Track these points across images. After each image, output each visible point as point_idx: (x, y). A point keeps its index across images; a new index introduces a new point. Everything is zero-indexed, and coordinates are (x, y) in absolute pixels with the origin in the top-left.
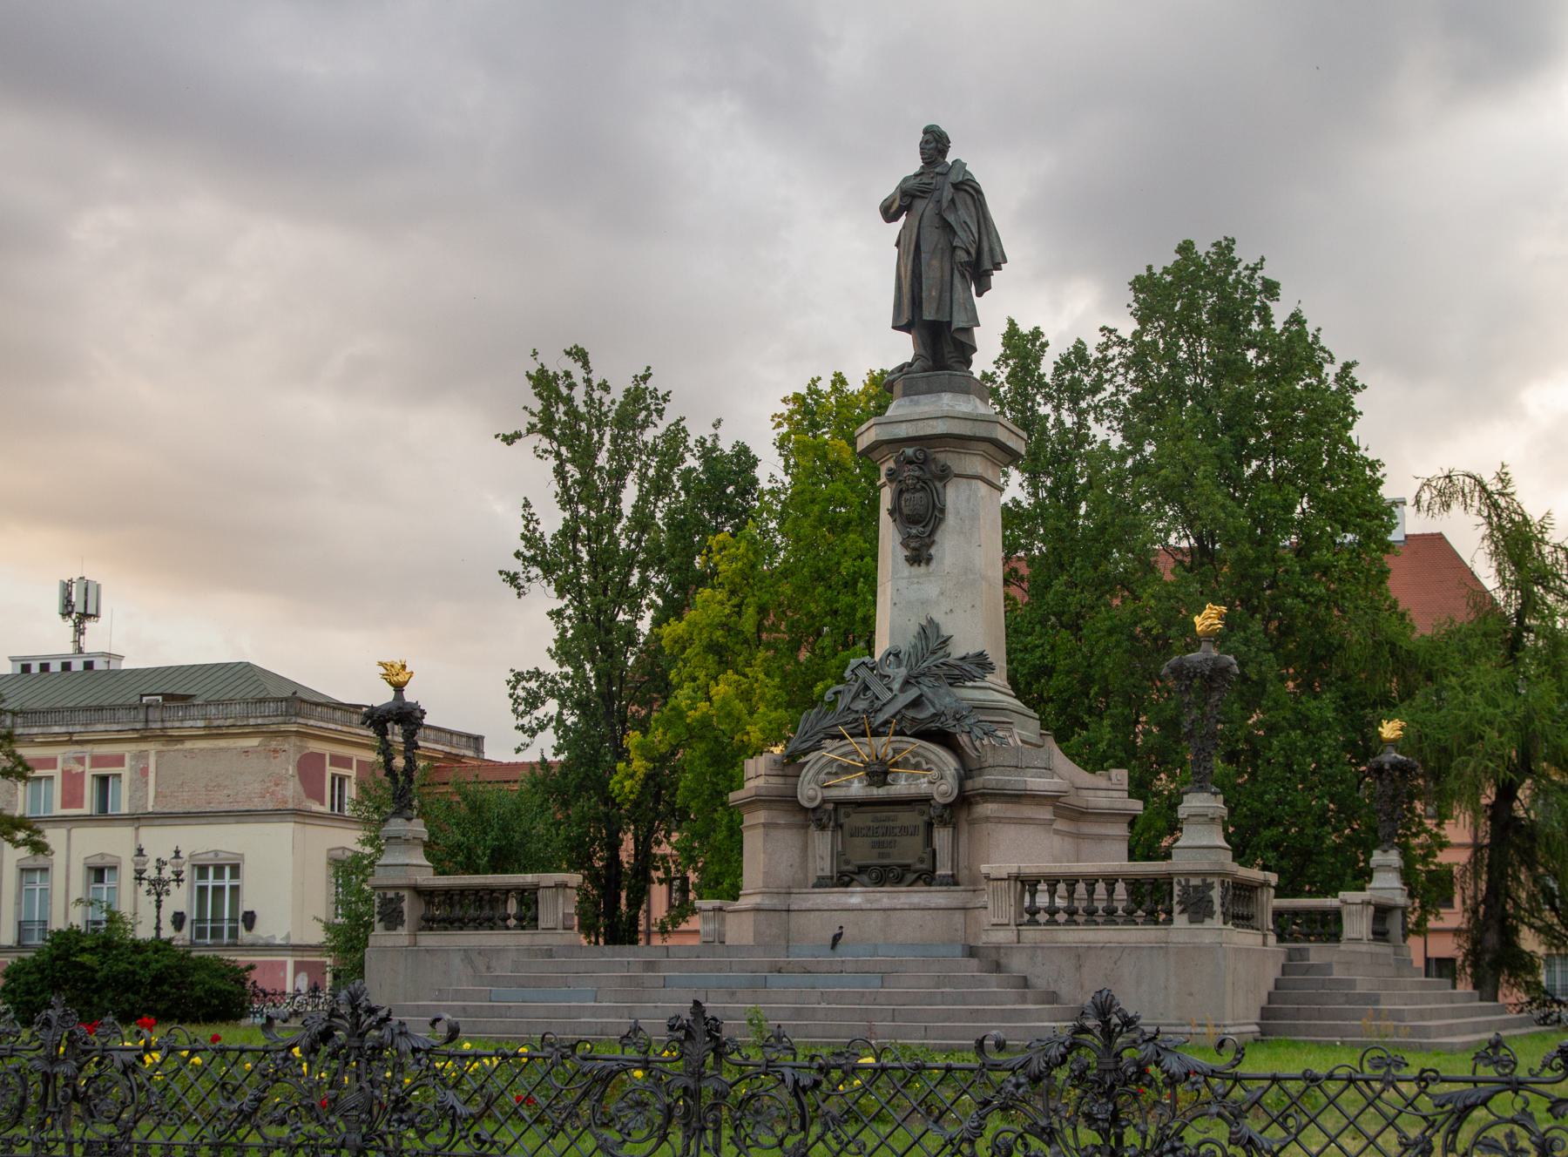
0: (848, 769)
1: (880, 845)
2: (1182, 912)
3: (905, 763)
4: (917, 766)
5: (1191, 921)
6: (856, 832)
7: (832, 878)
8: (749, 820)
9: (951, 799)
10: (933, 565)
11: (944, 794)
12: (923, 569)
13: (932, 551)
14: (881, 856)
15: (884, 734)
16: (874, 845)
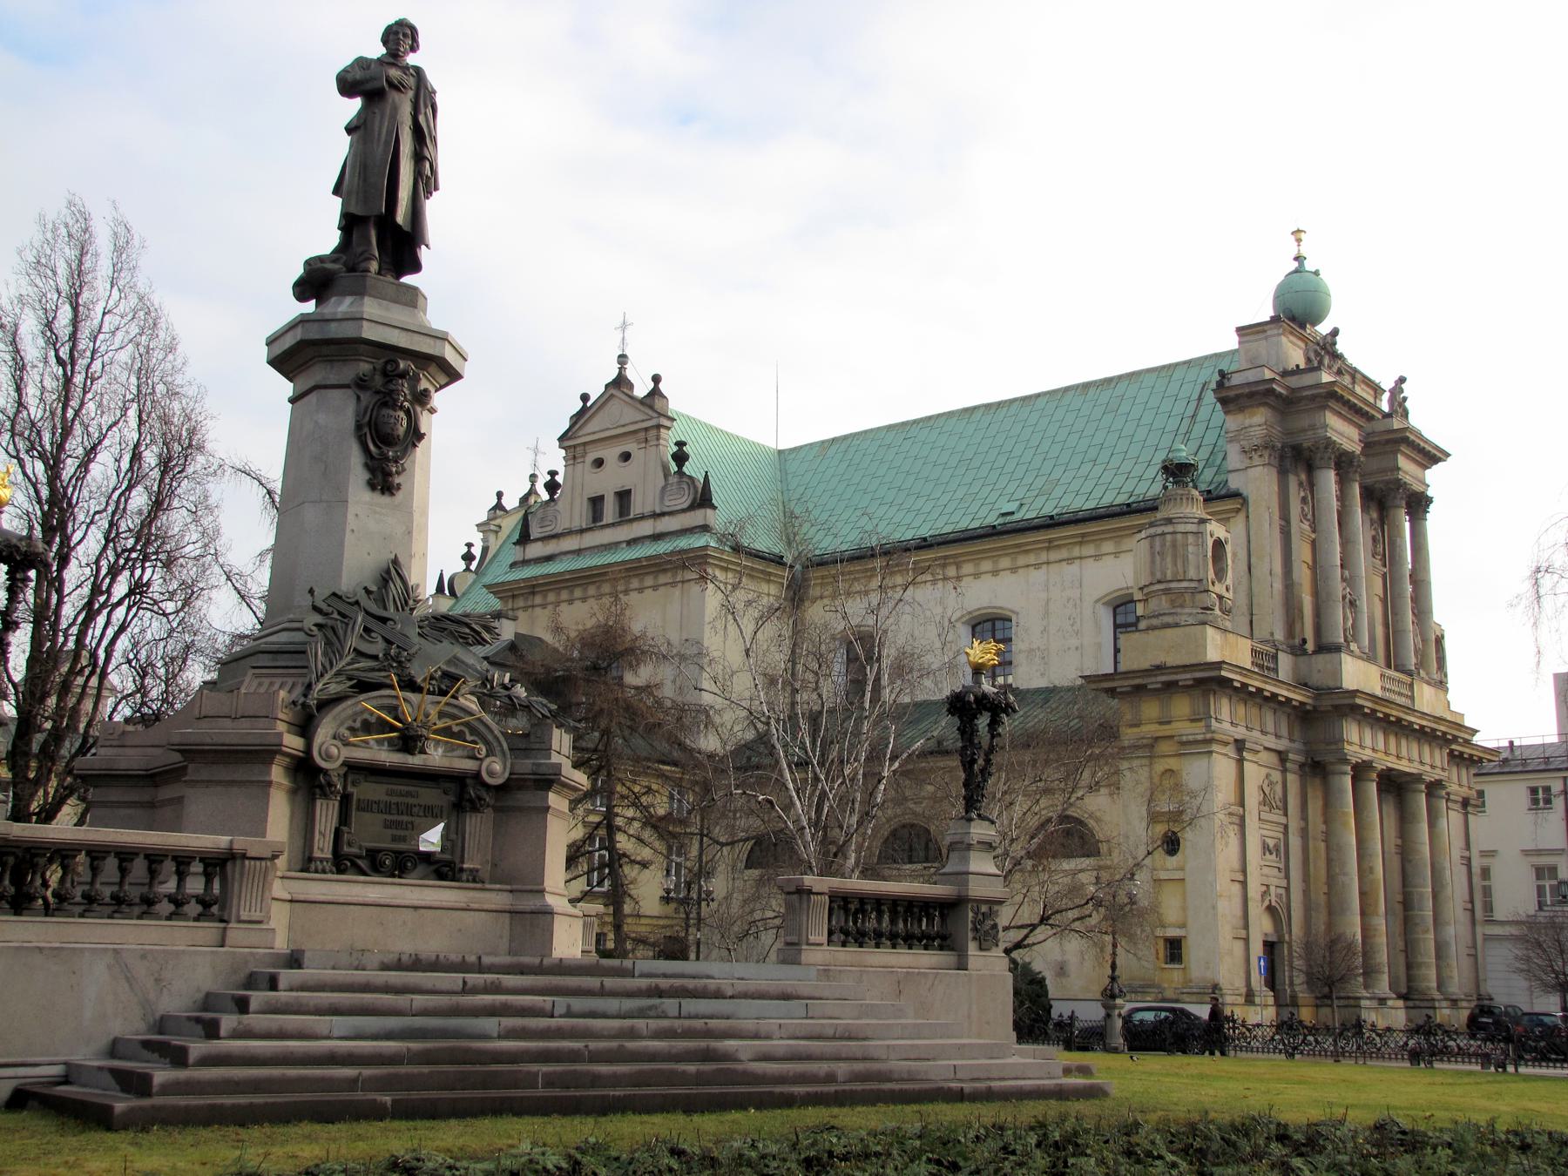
0: (384, 726)
1: (398, 825)
2: (974, 938)
3: (447, 731)
4: (460, 736)
5: (981, 949)
6: (366, 806)
7: (327, 860)
8: (193, 771)
9: (500, 781)
10: (400, 495)
11: (491, 774)
12: (386, 499)
13: (397, 480)
14: (395, 839)
15: (429, 693)
16: (388, 825)
